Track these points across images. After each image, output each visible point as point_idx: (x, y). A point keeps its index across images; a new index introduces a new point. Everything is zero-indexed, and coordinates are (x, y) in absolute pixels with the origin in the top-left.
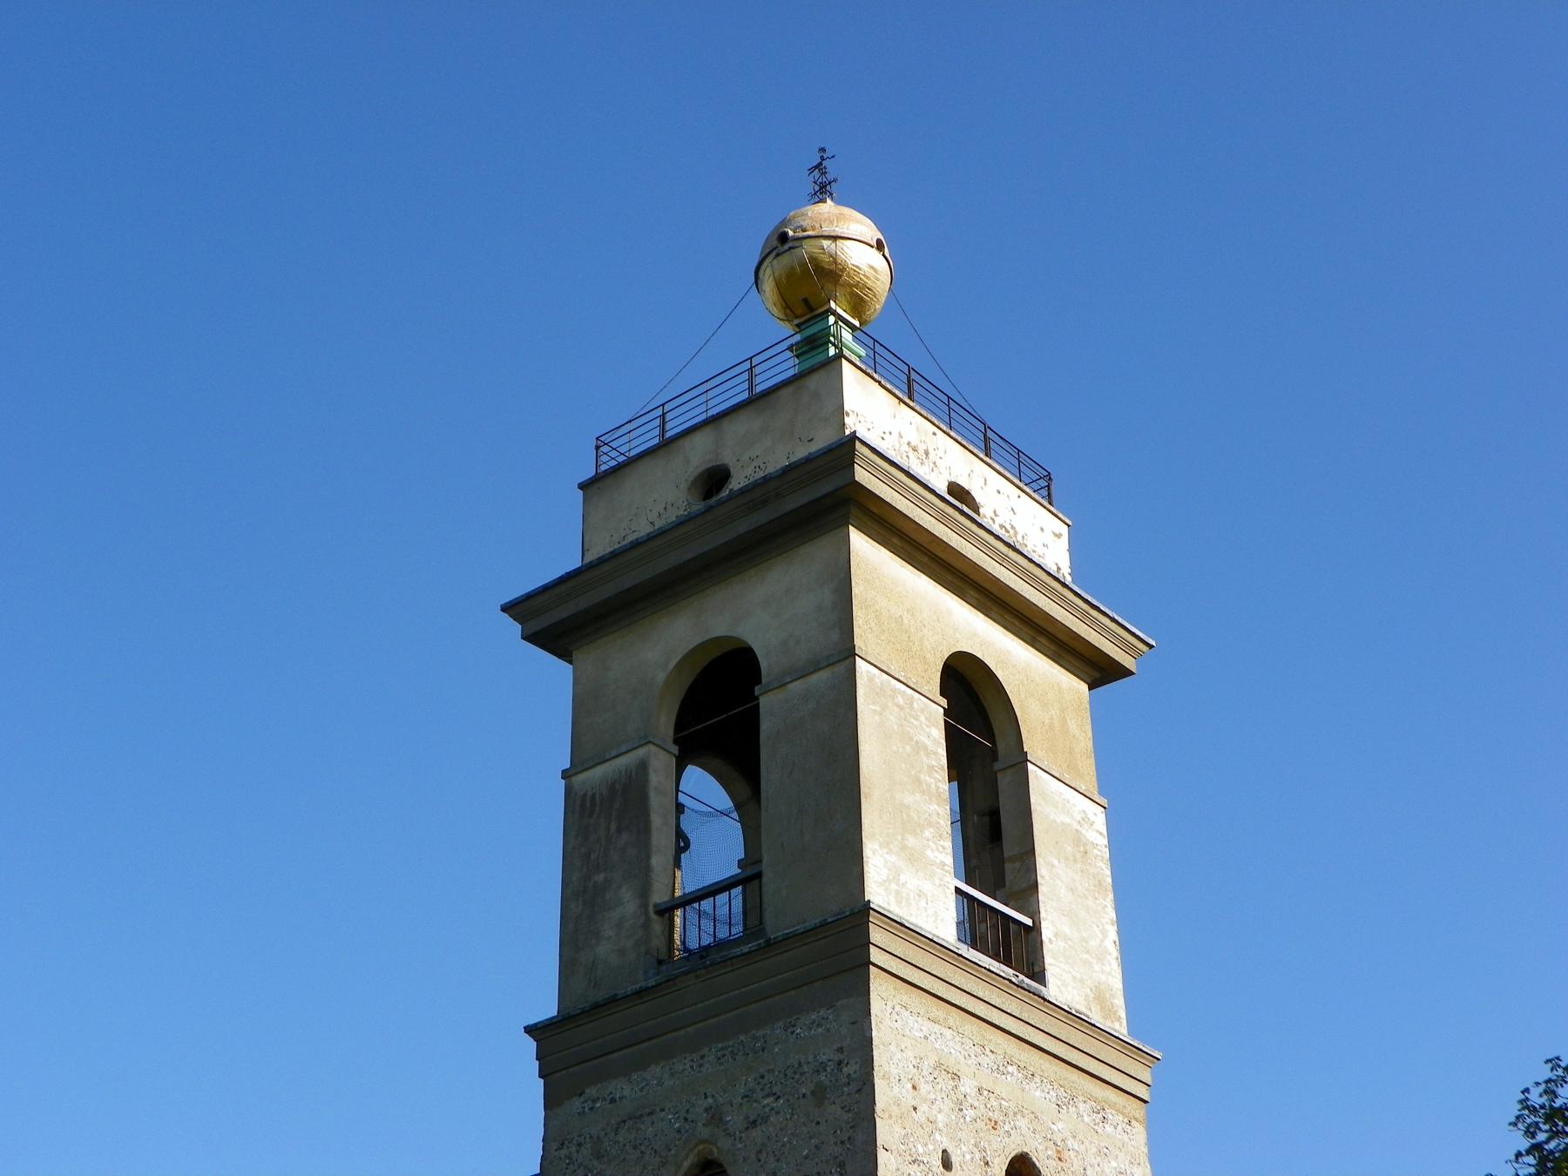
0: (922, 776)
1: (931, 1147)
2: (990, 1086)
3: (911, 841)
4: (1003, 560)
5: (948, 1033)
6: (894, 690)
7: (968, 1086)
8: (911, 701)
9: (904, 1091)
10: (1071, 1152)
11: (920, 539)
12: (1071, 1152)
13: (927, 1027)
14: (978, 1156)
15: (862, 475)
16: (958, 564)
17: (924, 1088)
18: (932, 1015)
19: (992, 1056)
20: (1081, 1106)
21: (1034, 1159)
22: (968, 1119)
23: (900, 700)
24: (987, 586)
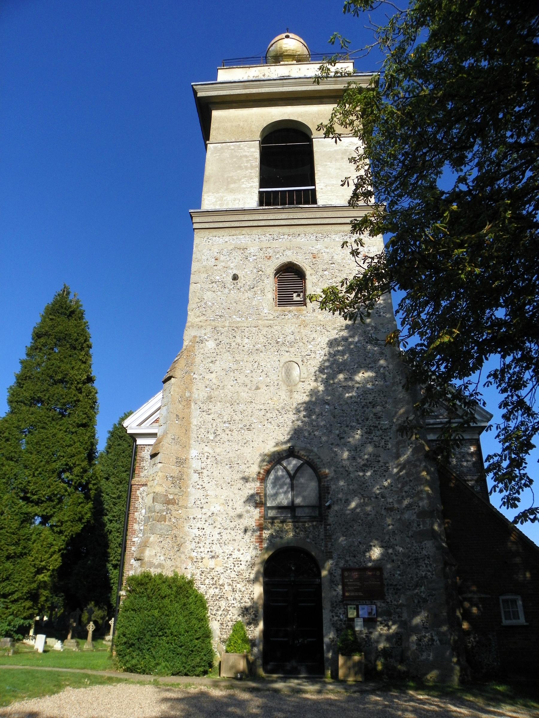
0: (242, 165)
1: (224, 275)
2: (269, 246)
3: (232, 186)
4: (283, 85)
5: (242, 237)
6: (230, 146)
7: (253, 250)
8: (239, 146)
9: (209, 263)
10: (324, 254)
11: (243, 98)
12: (324, 254)
13: (227, 239)
14: (255, 270)
15: (200, 94)
16: (265, 97)
17: (222, 258)
18: (232, 234)
19: (270, 236)
20: (333, 237)
21: (295, 262)
22: (251, 260)
23: (232, 147)
24: (284, 97)
